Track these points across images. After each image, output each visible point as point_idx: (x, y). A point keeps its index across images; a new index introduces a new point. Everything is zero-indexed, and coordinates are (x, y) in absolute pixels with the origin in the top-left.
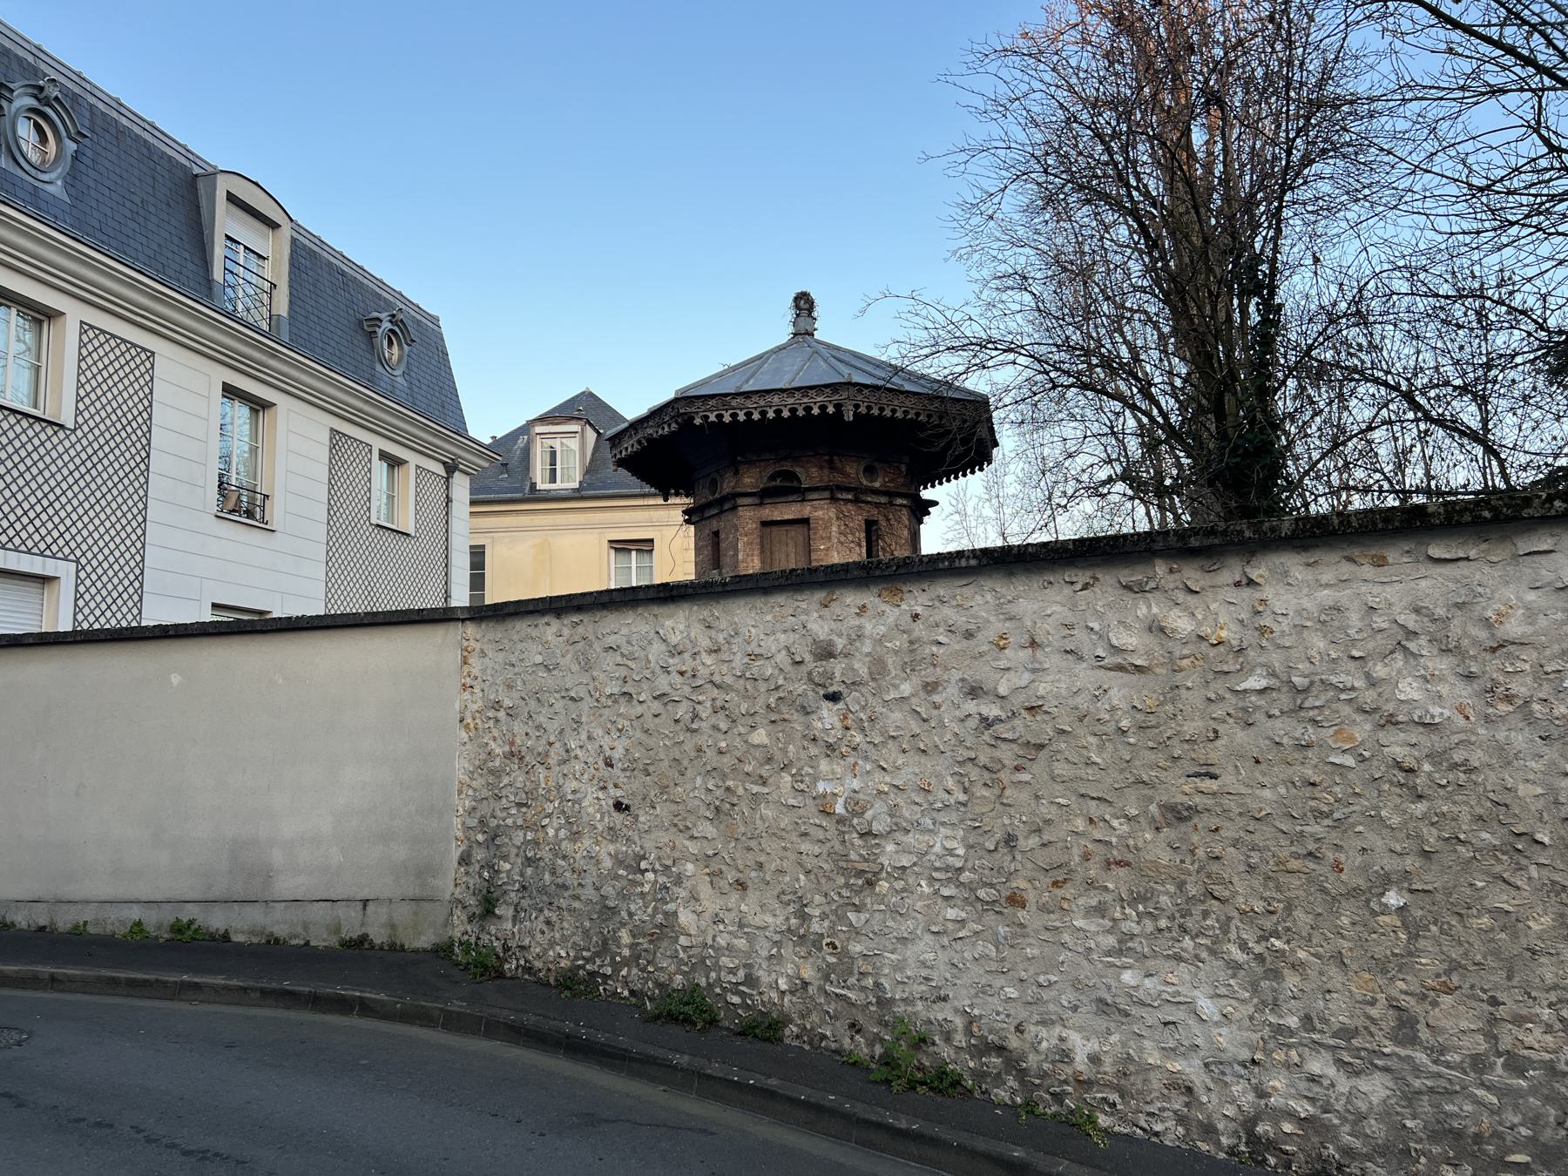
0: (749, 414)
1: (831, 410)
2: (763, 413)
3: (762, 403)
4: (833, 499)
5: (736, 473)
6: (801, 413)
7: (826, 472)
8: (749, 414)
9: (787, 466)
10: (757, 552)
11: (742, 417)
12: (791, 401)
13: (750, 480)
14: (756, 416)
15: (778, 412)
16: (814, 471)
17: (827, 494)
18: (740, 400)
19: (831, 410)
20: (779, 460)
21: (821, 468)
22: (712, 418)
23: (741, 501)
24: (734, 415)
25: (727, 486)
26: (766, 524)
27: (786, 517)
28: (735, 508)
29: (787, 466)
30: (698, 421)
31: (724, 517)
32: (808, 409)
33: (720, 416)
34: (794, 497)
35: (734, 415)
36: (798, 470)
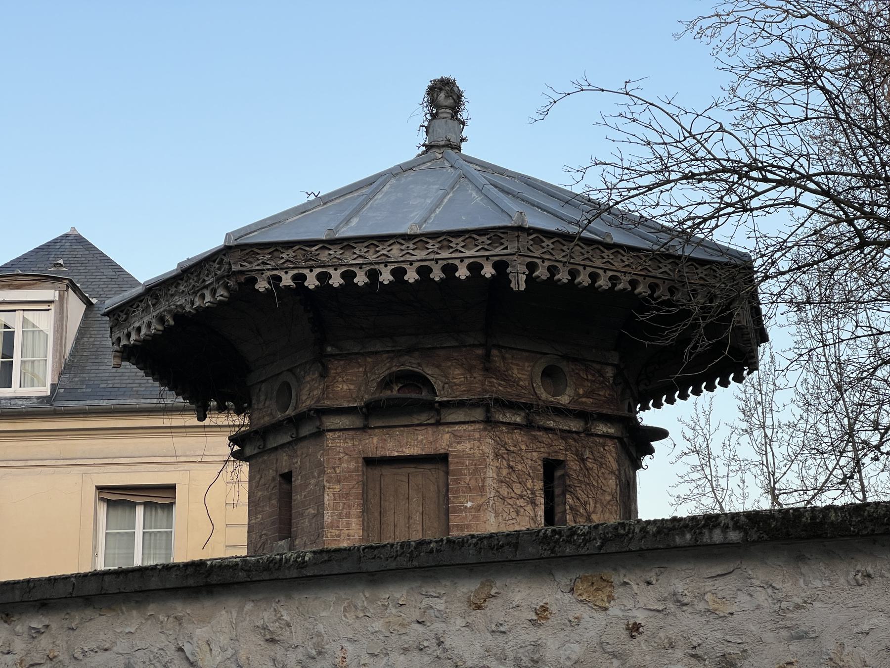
0: (348, 276)
1: (488, 271)
2: (373, 275)
3: (372, 257)
4: (489, 422)
5: (324, 375)
7: (478, 375)
8: (348, 276)
9: (411, 364)
10: (355, 511)
11: (336, 280)
12: (420, 254)
13: (348, 386)
15: (399, 273)
16: (457, 374)
17: (478, 414)
18: (335, 251)
19: (488, 271)
21: (470, 369)
23: (332, 422)
24: (323, 277)
25: (308, 395)
26: (370, 462)
27: (408, 451)
28: (319, 434)
29: (411, 364)
30: (262, 285)
32: (450, 269)
33: (299, 279)
34: (423, 418)
35: (323, 277)
36: (429, 371)
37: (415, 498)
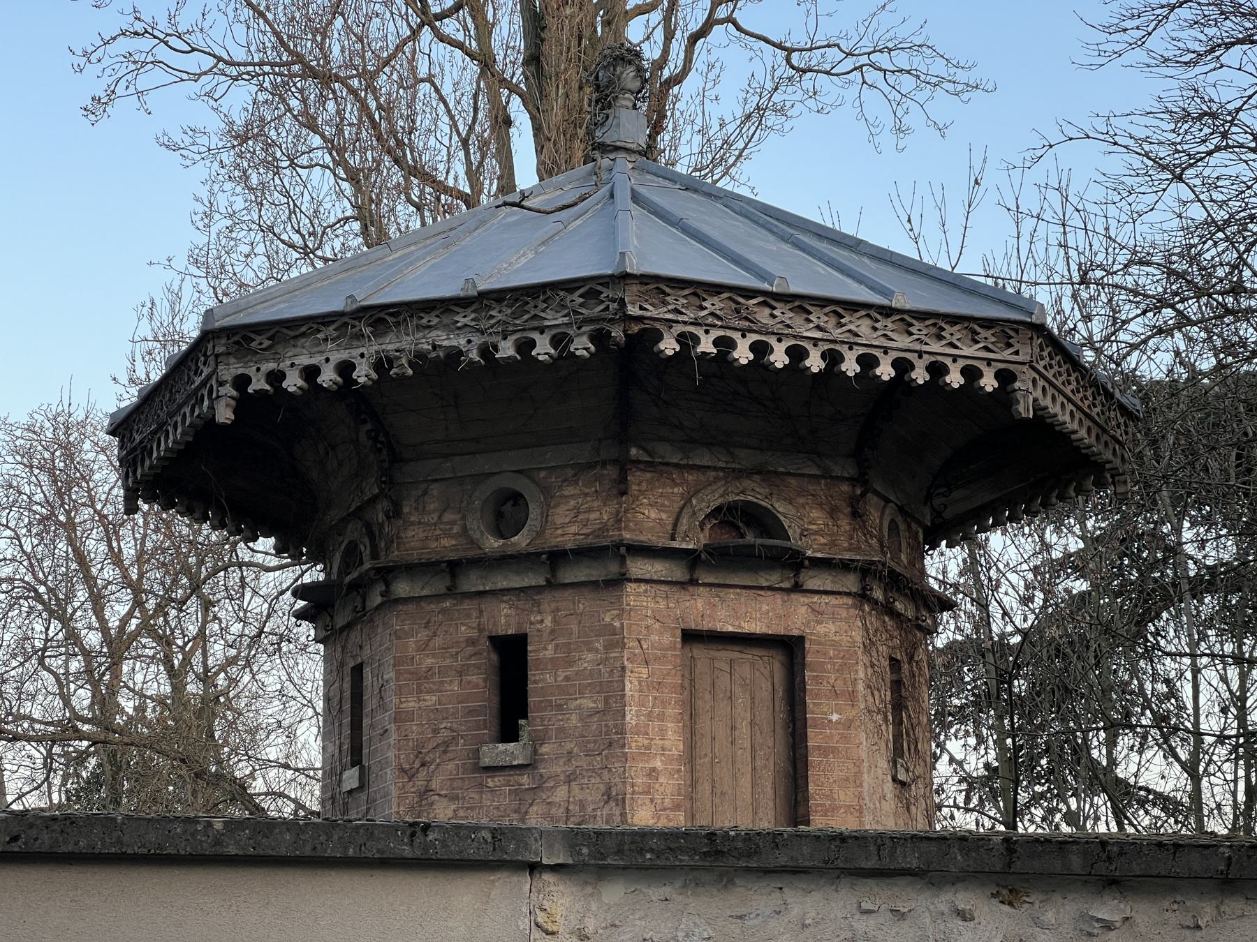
0: (797, 354)
1: (989, 382)
2: (833, 358)
3: (837, 333)
4: (863, 596)
5: (622, 489)
6: (920, 376)
7: (845, 524)
8: (797, 354)
9: (754, 493)
10: (672, 711)
11: (779, 358)
12: (903, 341)
13: (654, 512)
14: (815, 363)
15: (868, 362)
16: (817, 517)
17: (850, 582)
18: (783, 313)
19: (989, 382)
20: (740, 474)
21: (833, 513)
22: (706, 345)
23: (639, 567)
24: (760, 349)
25: (571, 516)
26: (691, 637)
27: (749, 627)
28: (620, 581)
29: (754, 493)
30: (669, 346)
31: (548, 601)
32: (937, 370)
33: (725, 344)
34: (774, 578)
35: (760, 349)
36: (780, 508)
37: (742, 700)
